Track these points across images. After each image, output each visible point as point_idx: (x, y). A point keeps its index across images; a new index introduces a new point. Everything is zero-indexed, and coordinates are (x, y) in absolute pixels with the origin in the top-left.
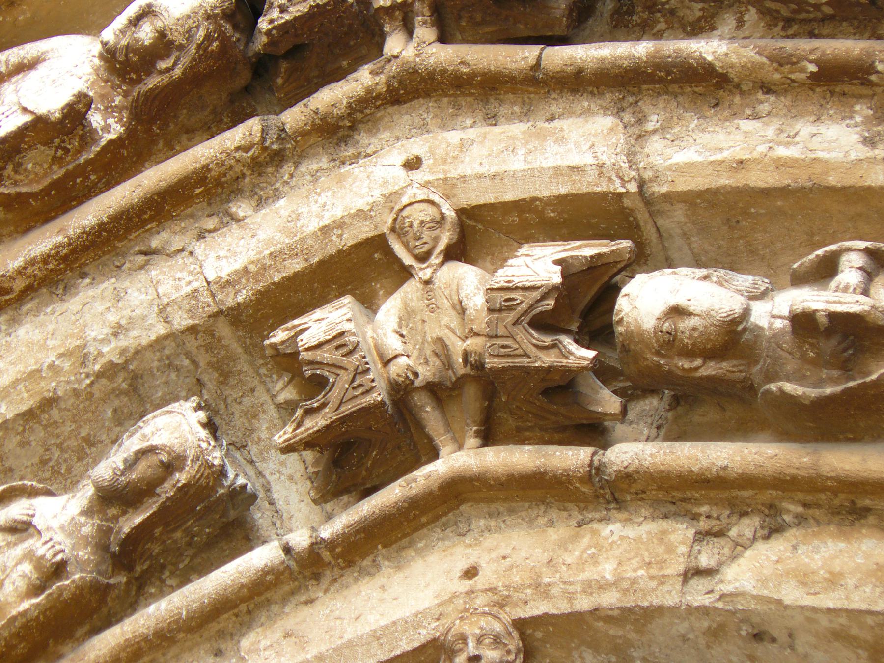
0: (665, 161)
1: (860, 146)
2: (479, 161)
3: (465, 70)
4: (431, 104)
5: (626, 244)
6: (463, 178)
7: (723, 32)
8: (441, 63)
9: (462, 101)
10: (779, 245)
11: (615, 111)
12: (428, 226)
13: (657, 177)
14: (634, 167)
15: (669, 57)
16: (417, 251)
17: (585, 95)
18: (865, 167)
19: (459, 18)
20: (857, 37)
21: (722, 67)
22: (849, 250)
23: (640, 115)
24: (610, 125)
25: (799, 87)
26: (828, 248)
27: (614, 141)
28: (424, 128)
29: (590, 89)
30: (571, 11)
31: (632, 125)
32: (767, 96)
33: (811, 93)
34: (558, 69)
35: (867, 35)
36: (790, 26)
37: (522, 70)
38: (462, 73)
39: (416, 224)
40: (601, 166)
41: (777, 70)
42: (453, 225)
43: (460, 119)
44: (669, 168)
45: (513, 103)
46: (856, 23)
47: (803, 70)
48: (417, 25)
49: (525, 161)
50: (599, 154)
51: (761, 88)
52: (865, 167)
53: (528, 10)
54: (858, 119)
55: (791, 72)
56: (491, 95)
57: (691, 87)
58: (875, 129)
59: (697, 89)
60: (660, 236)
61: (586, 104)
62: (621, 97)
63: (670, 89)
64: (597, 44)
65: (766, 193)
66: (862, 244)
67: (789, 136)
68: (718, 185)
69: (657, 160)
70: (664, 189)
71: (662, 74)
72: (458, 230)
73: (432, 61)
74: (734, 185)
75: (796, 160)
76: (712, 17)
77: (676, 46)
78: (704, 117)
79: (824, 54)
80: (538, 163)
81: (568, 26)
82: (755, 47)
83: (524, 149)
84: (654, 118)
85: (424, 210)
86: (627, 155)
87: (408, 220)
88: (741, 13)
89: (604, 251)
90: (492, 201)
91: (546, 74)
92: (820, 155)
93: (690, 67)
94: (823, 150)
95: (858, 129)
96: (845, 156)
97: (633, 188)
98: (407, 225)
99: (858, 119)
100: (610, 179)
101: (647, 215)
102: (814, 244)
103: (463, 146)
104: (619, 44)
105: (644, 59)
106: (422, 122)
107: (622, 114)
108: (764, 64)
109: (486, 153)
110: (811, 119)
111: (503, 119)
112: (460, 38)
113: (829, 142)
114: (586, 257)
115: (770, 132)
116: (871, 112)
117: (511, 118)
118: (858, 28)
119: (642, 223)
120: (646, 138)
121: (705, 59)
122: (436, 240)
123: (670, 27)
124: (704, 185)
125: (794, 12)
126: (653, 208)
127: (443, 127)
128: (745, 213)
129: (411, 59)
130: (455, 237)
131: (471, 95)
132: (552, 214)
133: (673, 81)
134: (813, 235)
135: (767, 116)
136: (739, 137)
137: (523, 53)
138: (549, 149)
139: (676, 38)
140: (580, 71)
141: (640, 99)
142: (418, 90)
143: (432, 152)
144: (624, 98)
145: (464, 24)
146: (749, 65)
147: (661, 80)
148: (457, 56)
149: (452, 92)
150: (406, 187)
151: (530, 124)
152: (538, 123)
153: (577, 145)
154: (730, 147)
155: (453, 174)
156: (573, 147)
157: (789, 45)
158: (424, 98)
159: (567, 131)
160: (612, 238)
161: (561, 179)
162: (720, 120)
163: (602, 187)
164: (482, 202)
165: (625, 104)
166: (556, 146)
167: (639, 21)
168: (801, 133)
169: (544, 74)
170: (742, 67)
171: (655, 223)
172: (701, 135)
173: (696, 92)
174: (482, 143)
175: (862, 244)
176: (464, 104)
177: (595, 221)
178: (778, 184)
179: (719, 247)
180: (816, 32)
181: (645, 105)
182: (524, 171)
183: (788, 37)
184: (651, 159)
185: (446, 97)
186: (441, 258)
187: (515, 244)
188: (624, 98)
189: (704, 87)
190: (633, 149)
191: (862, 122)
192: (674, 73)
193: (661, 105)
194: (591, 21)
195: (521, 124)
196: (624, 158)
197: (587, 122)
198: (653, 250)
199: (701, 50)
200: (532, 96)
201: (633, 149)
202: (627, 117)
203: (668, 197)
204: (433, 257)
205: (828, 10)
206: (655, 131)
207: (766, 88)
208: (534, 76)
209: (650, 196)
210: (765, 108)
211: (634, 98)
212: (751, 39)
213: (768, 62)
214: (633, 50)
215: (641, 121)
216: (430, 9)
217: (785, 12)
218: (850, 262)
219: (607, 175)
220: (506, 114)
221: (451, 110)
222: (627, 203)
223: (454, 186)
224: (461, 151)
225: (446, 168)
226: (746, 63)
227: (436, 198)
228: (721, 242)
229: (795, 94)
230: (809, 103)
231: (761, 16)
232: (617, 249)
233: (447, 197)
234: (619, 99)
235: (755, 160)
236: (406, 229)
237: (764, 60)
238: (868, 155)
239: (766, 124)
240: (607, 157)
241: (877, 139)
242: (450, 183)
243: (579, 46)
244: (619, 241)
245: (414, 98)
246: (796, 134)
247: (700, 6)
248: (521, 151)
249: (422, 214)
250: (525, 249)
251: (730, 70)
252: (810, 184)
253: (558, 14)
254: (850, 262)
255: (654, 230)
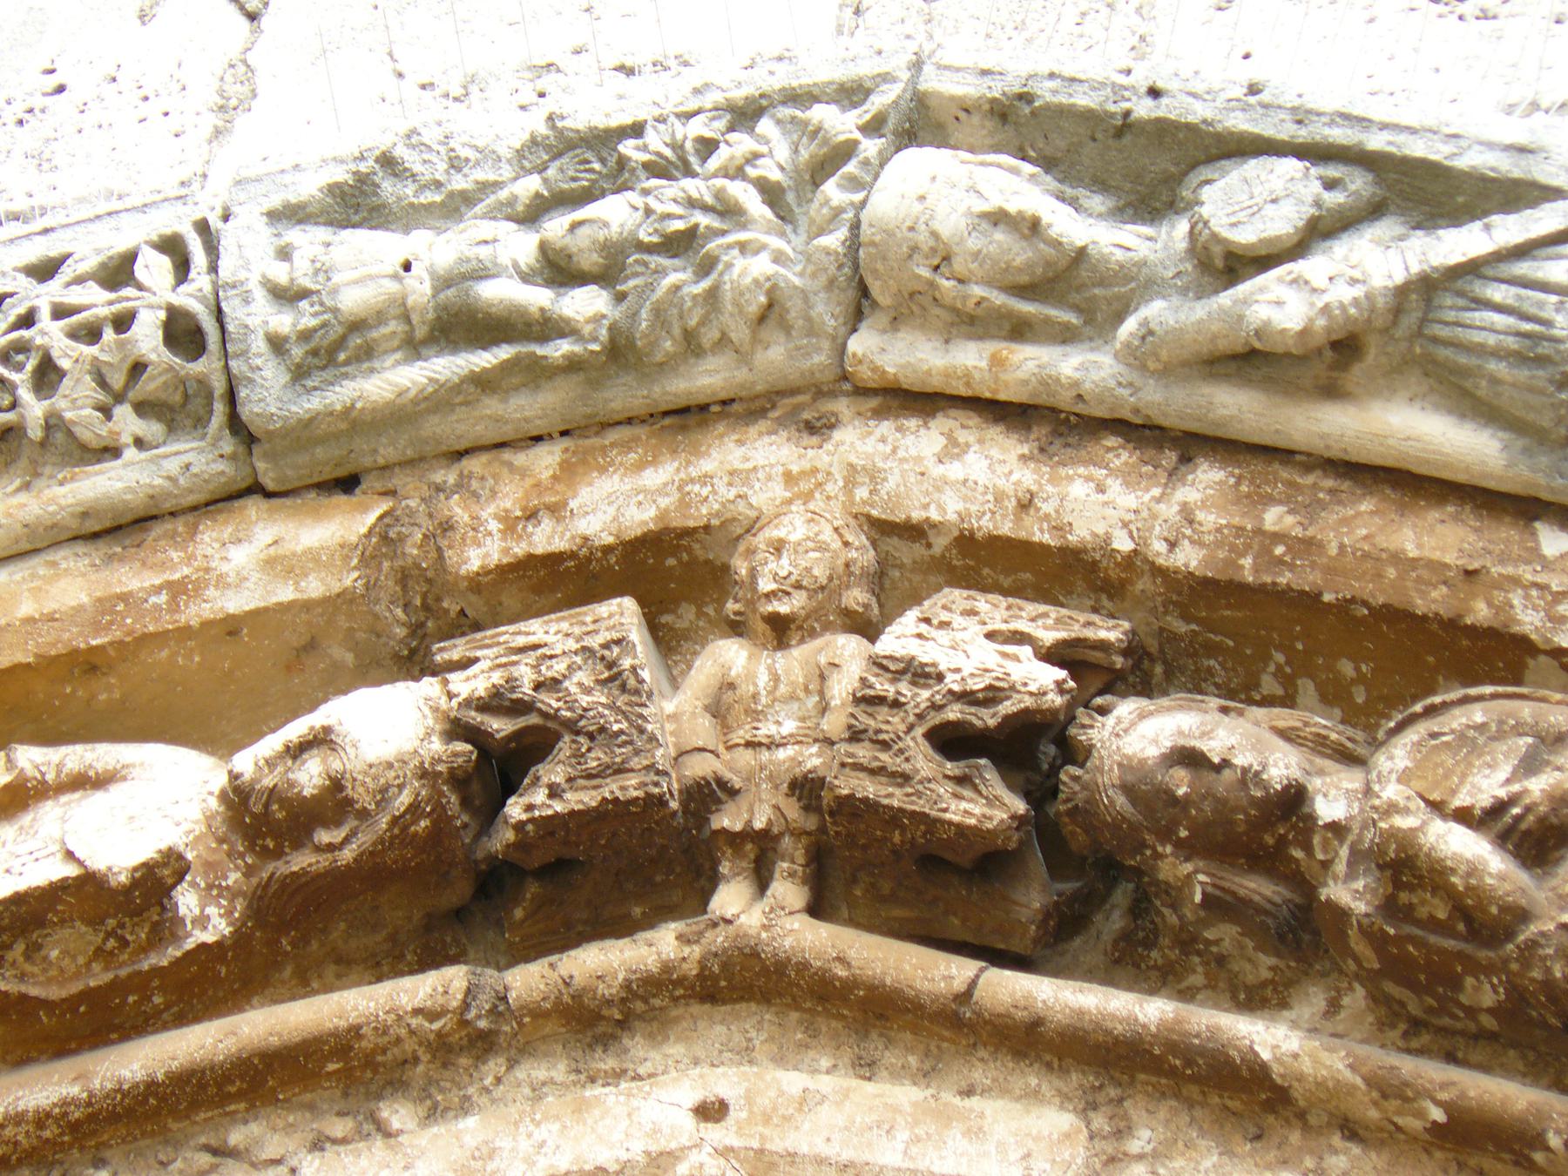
3: (841, 972)
4: (767, 1017)
6: (792, 1156)
9: (822, 1024)
19: (854, 880)
27: (1067, 1156)
28: (746, 1054)
29: (1048, 1057)
30: (1047, 915)
31: (1104, 1138)
34: (1001, 1010)
38: (835, 977)
43: (811, 1053)
45: (910, 1050)
48: (777, 875)
49: (905, 1153)
53: (975, 897)
56: (874, 1026)
61: (1033, 1081)
73: (788, 943)
80: (927, 1163)
81: (1036, 941)
91: (978, 1014)
103: (805, 1101)
107: (1091, 1114)
109: (841, 1124)
111: (885, 1073)
117: (899, 1074)
127: (780, 1060)
129: (753, 932)
131: (844, 1017)
137: (948, 967)
138: (950, 1142)
142: (751, 986)
143: (749, 1098)
145: (858, 893)
151: (930, 1091)
152: (943, 1094)
153: (1001, 1147)
155: (777, 1145)
158: (758, 1003)
159: (990, 1120)
165: (1101, 1098)
166: (965, 1142)
169: (974, 1012)
174: (839, 1104)
176: (824, 1029)
195: (915, 1088)
197: (1028, 1112)
200: (945, 1045)
202: (1100, 1121)
208: (956, 1013)
224: (800, 1110)
225: (767, 1132)
234: (1093, 1087)
245: (741, 999)
248: (903, 1135)
253: (1024, 915)
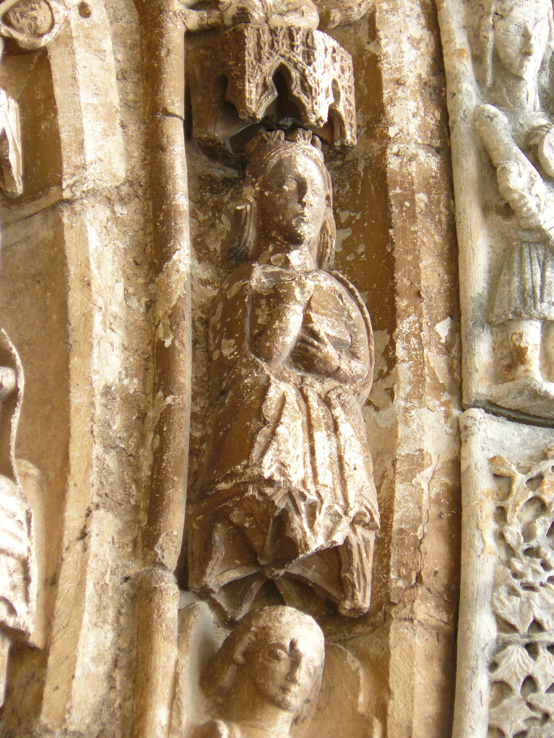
0: (89, 220)
1: (103, 384)
2: (87, 65)
3: (163, 53)
4: (134, 24)
5: (19, 189)
6: (73, 52)
7: (196, 268)
8: (169, 33)
9: (137, 51)
10: (20, 317)
11: (130, 179)
12: (33, 23)
13: (75, 214)
14: (84, 195)
15: (175, 223)
16: (11, 14)
17: (143, 154)
18: (86, 388)
19: (206, 48)
20: (194, 380)
21: (167, 267)
22: (17, 375)
23: (127, 200)
24: (118, 175)
25: (152, 331)
26: (18, 357)
27: (106, 178)
28: (114, 20)
29: (148, 158)
30: (213, 141)
31: (118, 193)
32: (144, 305)
33: (147, 342)
34: (165, 131)
35: (196, 388)
36: (202, 324)
37: (163, 100)
38: (160, 51)
39: (34, 13)
40: (84, 167)
41: (166, 313)
42: (33, 44)
43: (122, 49)
44: (83, 225)
45: (136, 94)
46: (205, 379)
47: (166, 335)
48: (200, 12)
49: (88, 104)
50: (94, 166)
51: (151, 301)
52: (86, 388)
53: (213, 105)
54: (126, 382)
55: (164, 325)
56: (142, 75)
57: (151, 242)
58: (118, 395)
59: (149, 247)
60: (26, 218)
61: (136, 154)
62: (142, 183)
63: (148, 225)
64: (185, 163)
65: (63, 306)
66: (21, 386)
67: (111, 324)
68: (70, 266)
69: (89, 215)
70: (65, 220)
71: (161, 218)
72: (29, 48)
73: (170, 25)
74: (69, 278)
75: (91, 330)
76: (210, 259)
77: (184, 229)
78: (126, 254)
79: (180, 352)
80: (86, 115)
81: (200, 139)
82: (184, 295)
83: (97, 103)
84: (125, 212)
85: (45, 20)
86: (93, 190)
87: (37, 6)
88: (213, 283)
89: (13, 171)
90: (54, 77)
91: (160, 121)
92: (96, 350)
93: (167, 241)
94: (99, 352)
95: (117, 382)
96: (94, 371)
97: (67, 194)
98: (33, 5)
99: (126, 382)
100: (73, 175)
101: (44, 206)
102: (21, 346)
103: (100, 52)
104: (186, 181)
105: (174, 203)
106: (118, 17)
107: (127, 185)
108: (170, 302)
109: (94, 71)
110: (125, 342)
111: (122, 85)
112: (189, 49)
113: (106, 358)
114: (8, 156)
115: (115, 309)
116: (131, 392)
117: (123, 92)
118: (202, 380)
119: (37, 202)
120: (108, 205)
121: (174, 253)
122: (21, 30)
123: (200, 224)
124: (69, 253)
125: (215, 327)
126: (49, 211)
127: (115, 36)
128: (46, 289)
129: (171, 8)
130: (23, 46)
131: (143, 60)
132: (43, 127)
133: (155, 227)
134: (29, 345)
135: (128, 305)
136: (110, 283)
137: (178, 102)
138: (98, 123)
139: (191, 229)
140: (163, 149)
141: (140, 200)
142: (146, 14)
143: (95, 26)
144: (141, 186)
145: (201, 52)
146: (169, 290)
147: (156, 217)
148: (174, 46)
149: (144, 42)
150: (65, 5)
151: (119, 108)
152: (119, 114)
153: (102, 147)
154: (101, 275)
155: (76, 44)
156: (100, 144)
157: (186, 324)
158: (139, 19)
159: (113, 139)
160: (25, 178)
161: (73, 134)
162: (124, 266)
163: (67, 168)
164: (53, 68)
165: (136, 187)
166: (100, 130)
167: (205, 198)
168: (113, 334)
169: (160, 119)
170: (168, 284)
171: (37, 213)
172: (111, 251)
173: (146, 246)
174: (103, 68)
175: (21, 386)
176: (135, 52)
177: (39, 163)
178: (70, 316)
179: (18, 267)
180: (198, 346)
181: (135, 204)
182: (79, 103)
183: (193, 322)
184: (90, 209)
185: (141, 37)
186: (6, 35)
187: (18, 96)
188: (141, 186)
189: (151, 252)
190: (98, 194)
191: (123, 385)
192: (162, 228)
193: (136, 217)
194: (205, 158)
195: (118, 100)
196: (91, 187)
197: (121, 155)
198: (14, 212)
199: (181, 251)
200: (142, 109)
201: (98, 194)
202: (125, 189)
203: (58, 225)
204: (6, 27)
205: (216, 355)
206: (114, 212)
207: (151, 304)
208: (158, 111)
209: (59, 209)
210: (134, 303)
211: (141, 194)
212: (190, 291)
213: (172, 305)
214: (181, 193)
215: (122, 200)
216: (214, 24)
217: (214, 319)
218: (7, 376)
219: (77, 172)
220: (127, 87)
221: (129, 41)
222: (54, 189)
223: (66, 45)
224: (95, 51)
225: (81, 38)
226: (171, 287)
227: (55, 30)
228: (22, 268)
229: (146, 329)
230: (139, 340)
231: (211, 300)
232: (15, 181)
233: (57, 39)
234: (140, 182)
235: (91, 296)
236: (29, 5)
237: (174, 303)
238: (96, 390)
239: (120, 305)
240: (91, 173)
241: (109, 397)
242: (69, 41)
243: (184, 148)
244: (21, 183)
245: (139, 10)
246: (113, 330)
247: (219, 249)
248: (96, 101)
249: (42, 18)
250: (14, 105)
251: (165, 274)
252: (71, 342)
253: (211, 130)
254: (7, 376)
255: (31, 212)
